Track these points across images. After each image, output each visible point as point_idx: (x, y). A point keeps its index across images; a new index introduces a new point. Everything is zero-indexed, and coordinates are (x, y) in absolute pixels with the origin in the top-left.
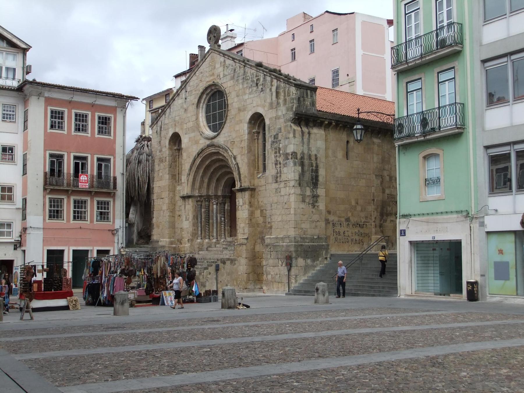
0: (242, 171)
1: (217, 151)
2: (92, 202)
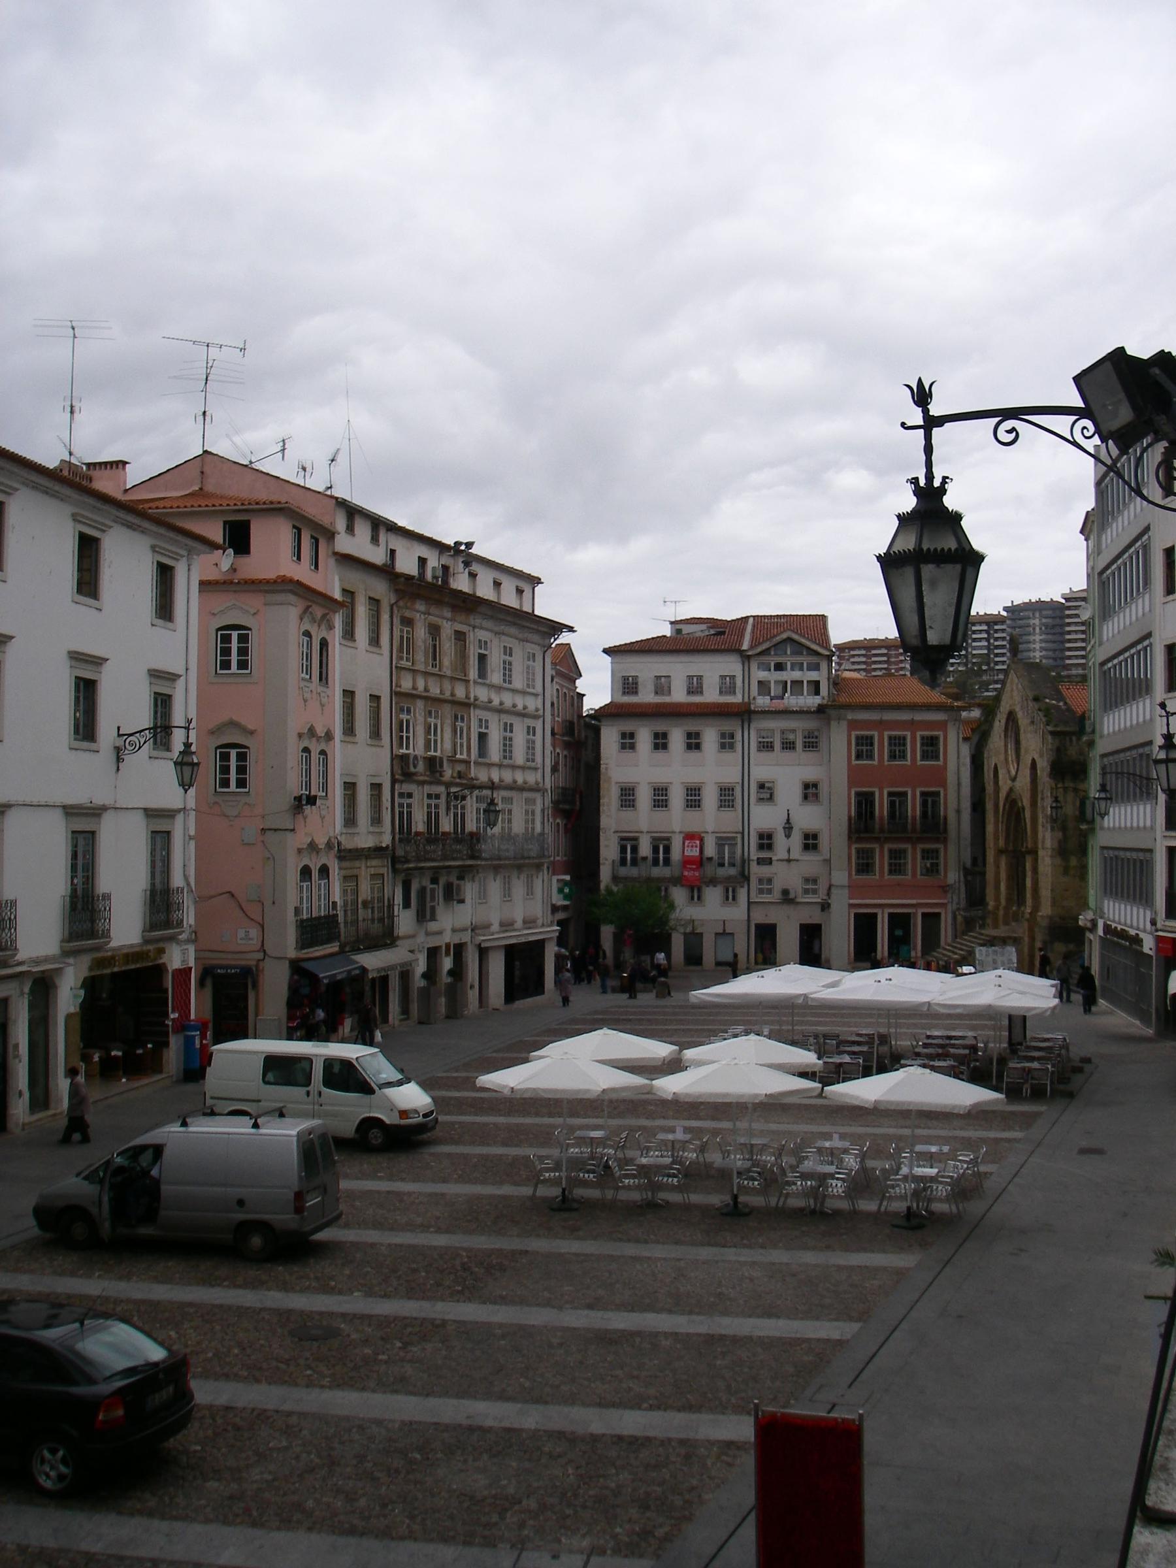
2: (914, 849)
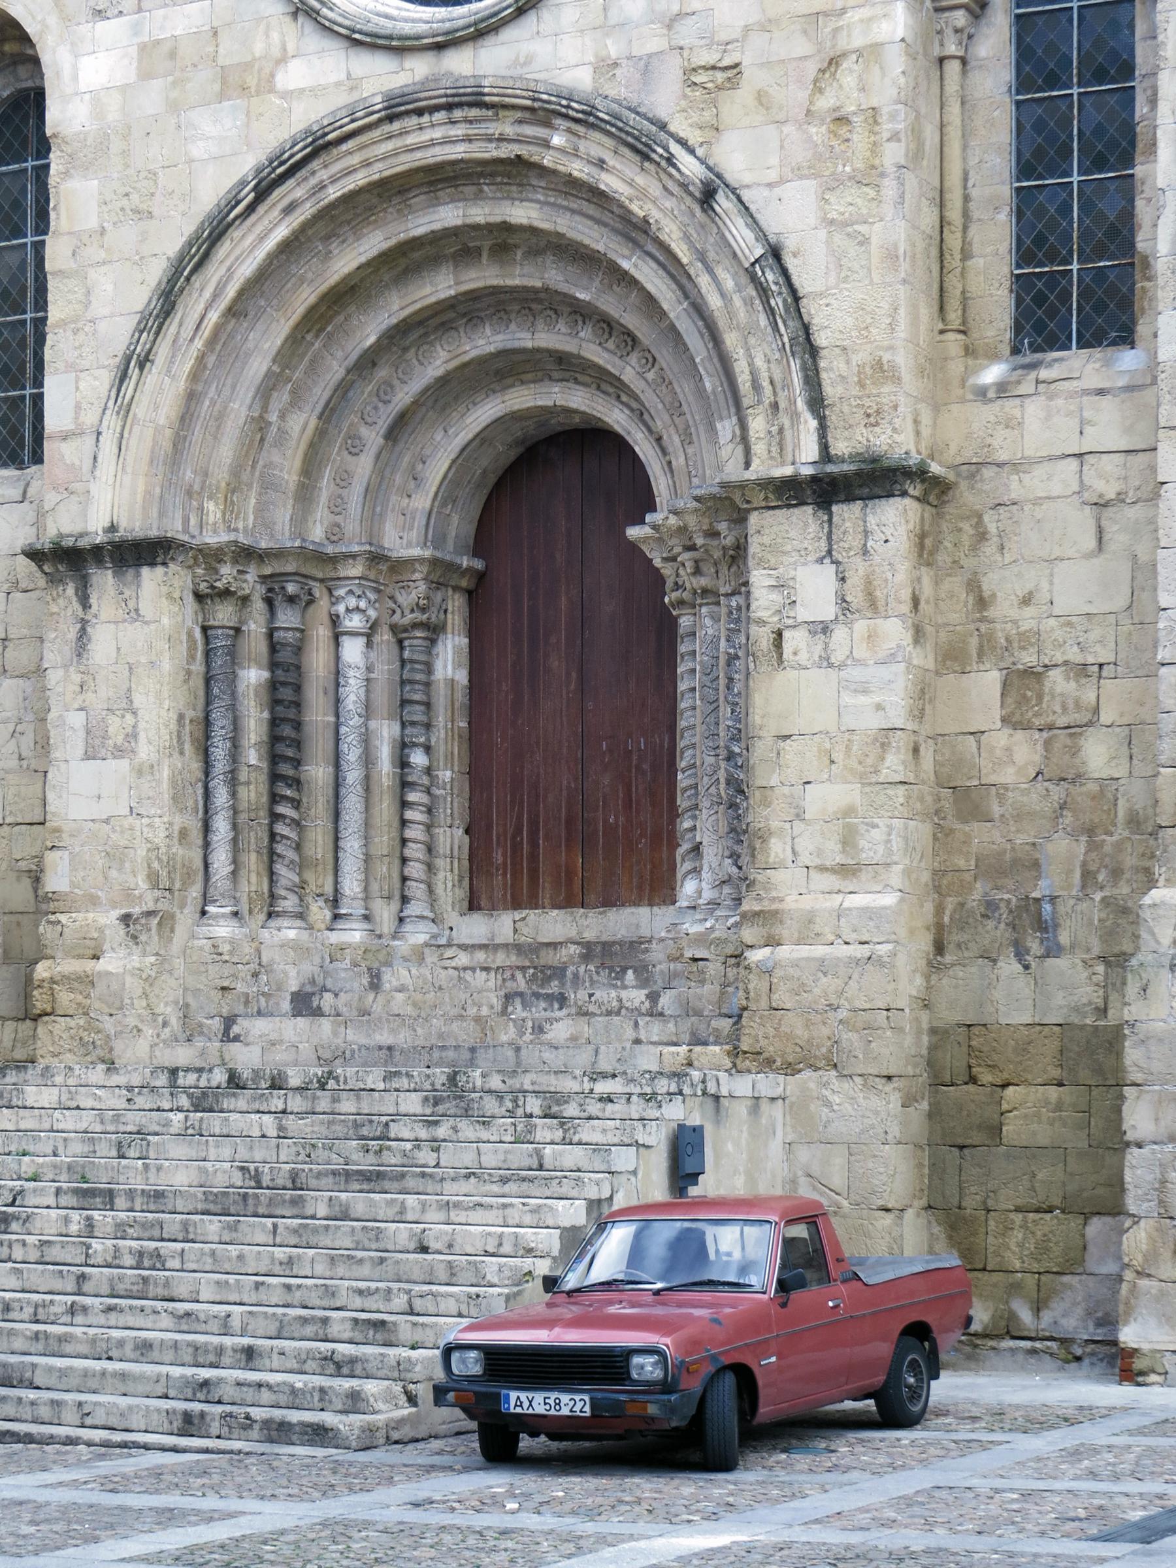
0: (831, 322)
1: (505, 151)
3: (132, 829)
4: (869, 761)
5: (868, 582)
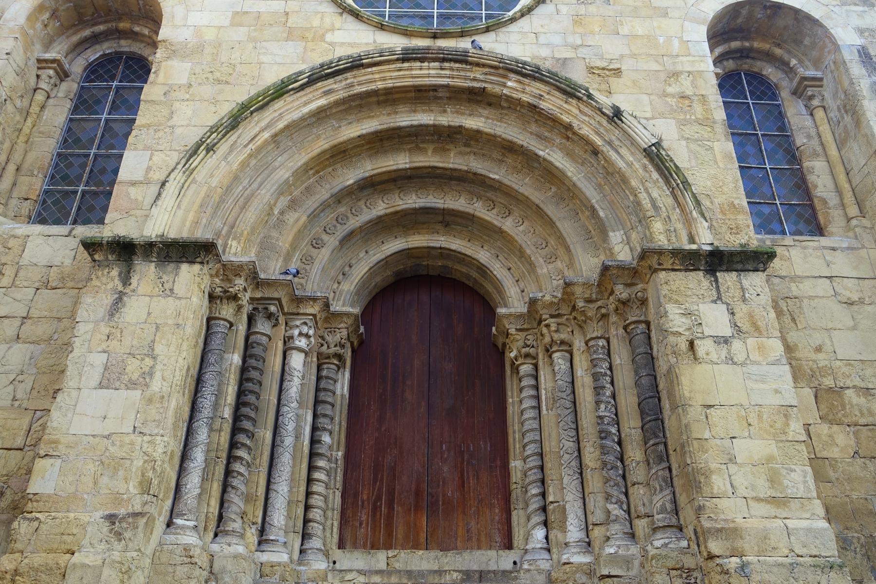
3: (132, 443)
4: (778, 425)
5: (751, 316)
